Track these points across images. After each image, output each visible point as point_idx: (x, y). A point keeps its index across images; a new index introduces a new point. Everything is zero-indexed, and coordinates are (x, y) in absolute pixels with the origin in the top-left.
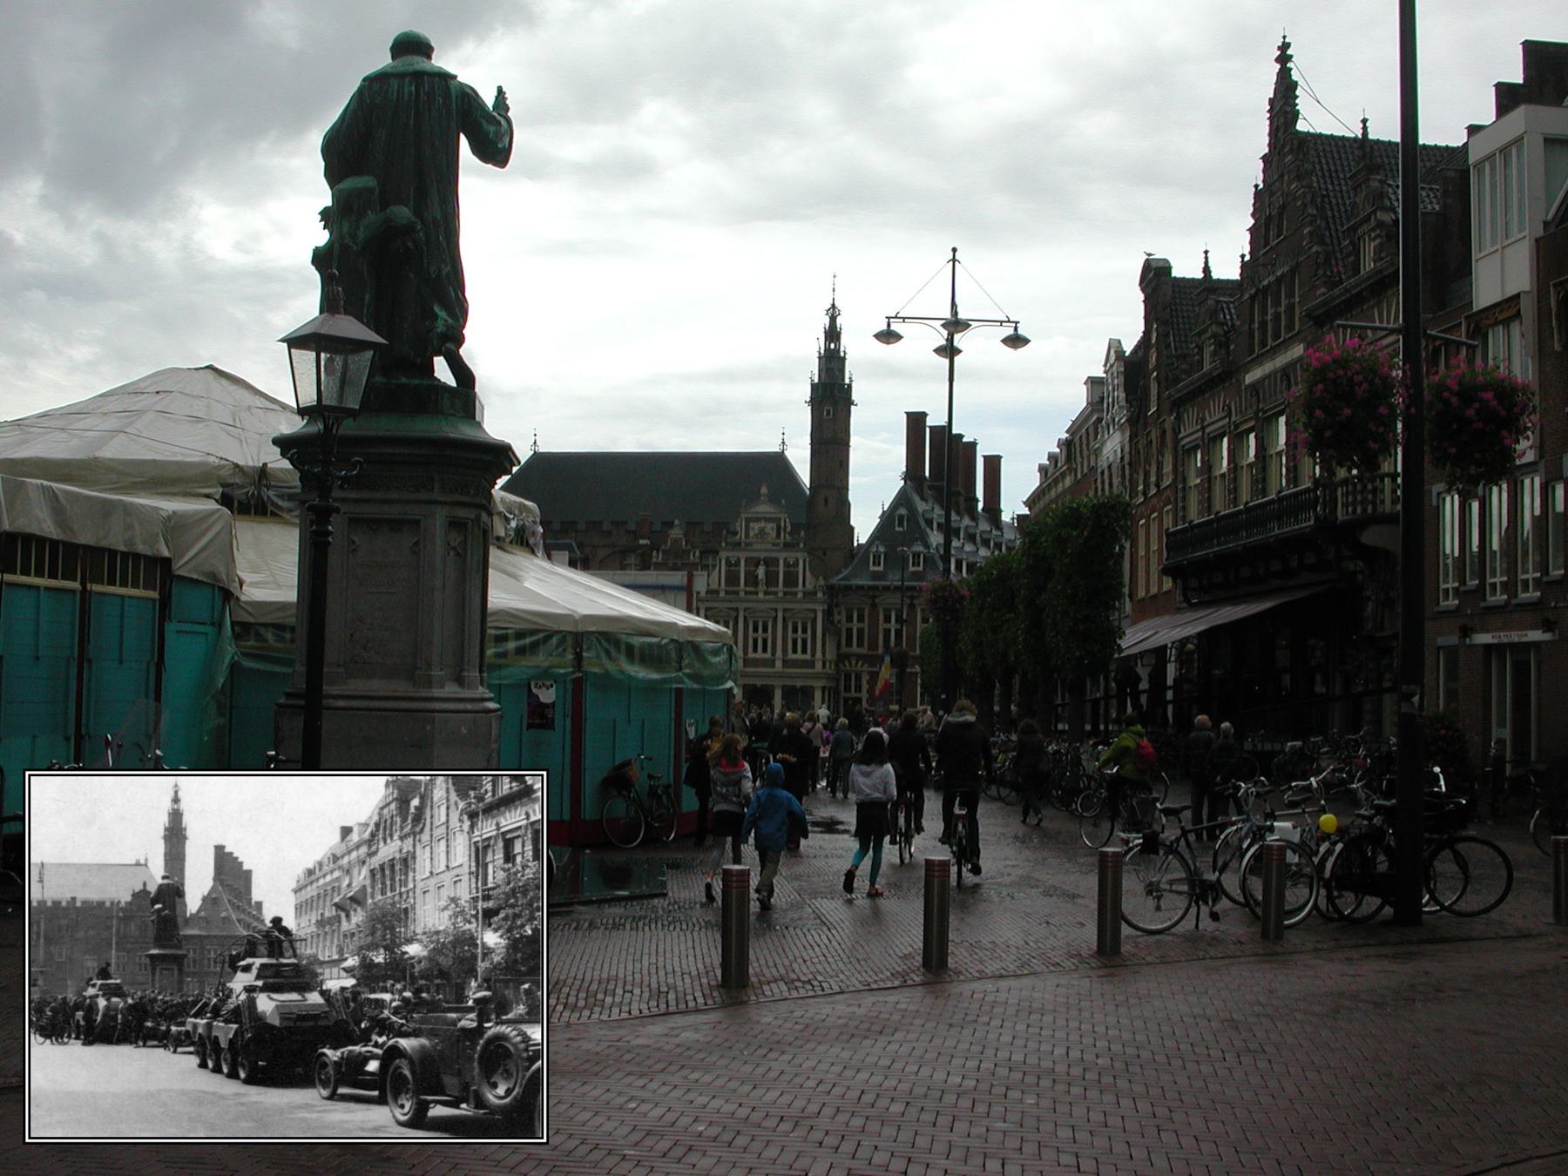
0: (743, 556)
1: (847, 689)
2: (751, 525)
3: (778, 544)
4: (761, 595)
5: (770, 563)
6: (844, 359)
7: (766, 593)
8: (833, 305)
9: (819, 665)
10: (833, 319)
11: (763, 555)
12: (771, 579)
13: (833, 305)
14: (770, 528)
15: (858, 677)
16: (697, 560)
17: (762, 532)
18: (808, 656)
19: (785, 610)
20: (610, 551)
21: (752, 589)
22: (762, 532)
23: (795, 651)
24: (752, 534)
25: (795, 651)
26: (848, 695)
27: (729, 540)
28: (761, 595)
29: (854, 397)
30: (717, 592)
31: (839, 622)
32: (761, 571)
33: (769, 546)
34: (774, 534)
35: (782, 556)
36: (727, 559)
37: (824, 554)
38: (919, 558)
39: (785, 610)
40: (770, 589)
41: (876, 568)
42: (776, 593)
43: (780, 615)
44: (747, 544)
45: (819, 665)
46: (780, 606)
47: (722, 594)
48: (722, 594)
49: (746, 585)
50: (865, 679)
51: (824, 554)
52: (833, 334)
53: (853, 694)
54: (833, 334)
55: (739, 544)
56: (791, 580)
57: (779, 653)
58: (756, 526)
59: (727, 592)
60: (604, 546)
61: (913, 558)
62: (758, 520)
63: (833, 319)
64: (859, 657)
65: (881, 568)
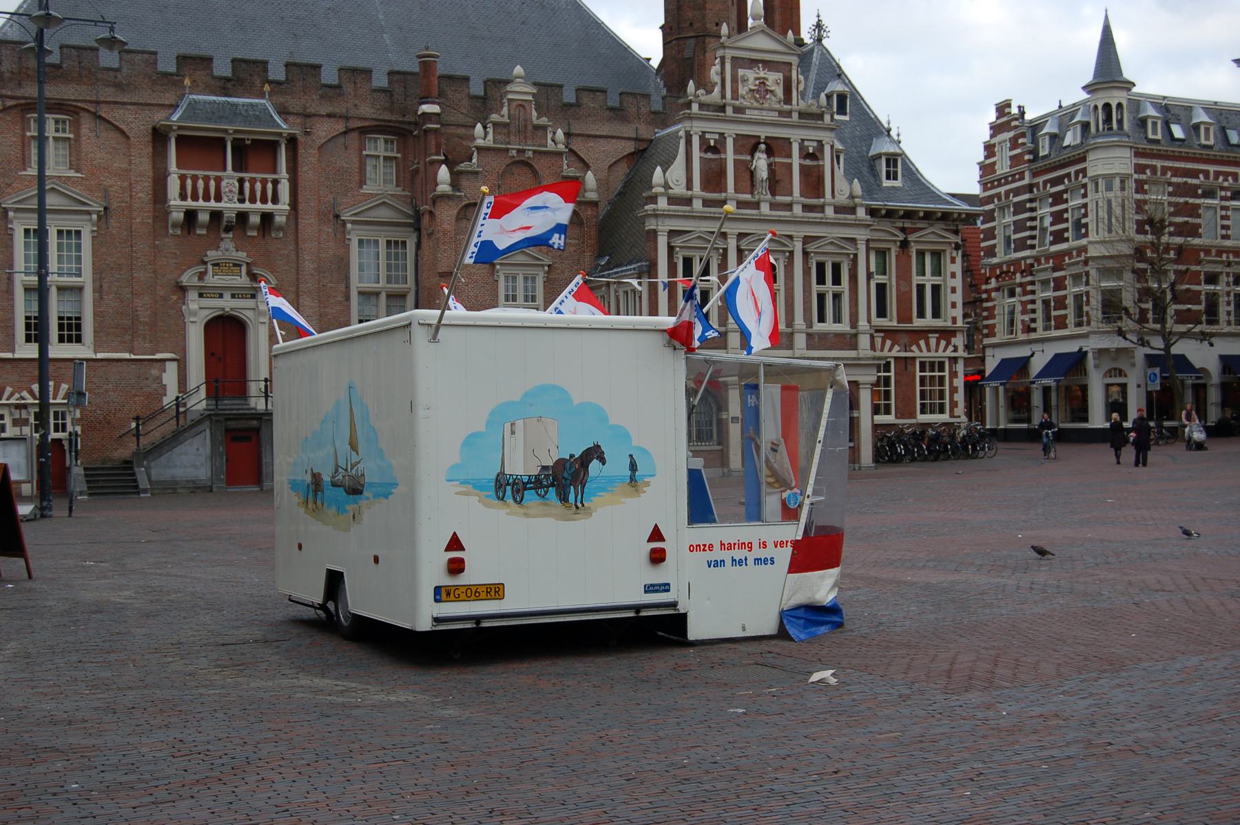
0: (731, 130)
2: (741, 72)
3: (789, 114)
4: (765, 209)
5: (774, 147)
7: (774, 206)
9: (864, 341)
11: (763, 132)
12: (776, 182)
14: (774, 79)
16: (561, 147)
17: (762, 88)
18: (844, 327)
19: (807, 240)
20: (340, 127)
21: (747, 197)
22: (762, 88)
23: (822, 319)
24: (742, 91)
25: (822, 319)
27: (705, 99)
28: (765, 209)
30: (688, 201)
32: (761, 163)
33: (774, 116)
34: (780, 92)
35: (795, 135)
36: (702, 138)
39: (807, 240)
40: (779, 198)
42: (789, 206)
43: (798, 247)
44: (738, 110)
45: (864, 341)
46: (800, 232)
47: (697, 205)
48: (697, 205)
49: (736, 191)
55: (722, 108)
56: (814, 182)
57: (799, 321)
58: (750, 74)
59: (706, 203)
60: (329, 116)
62: (753, 63)
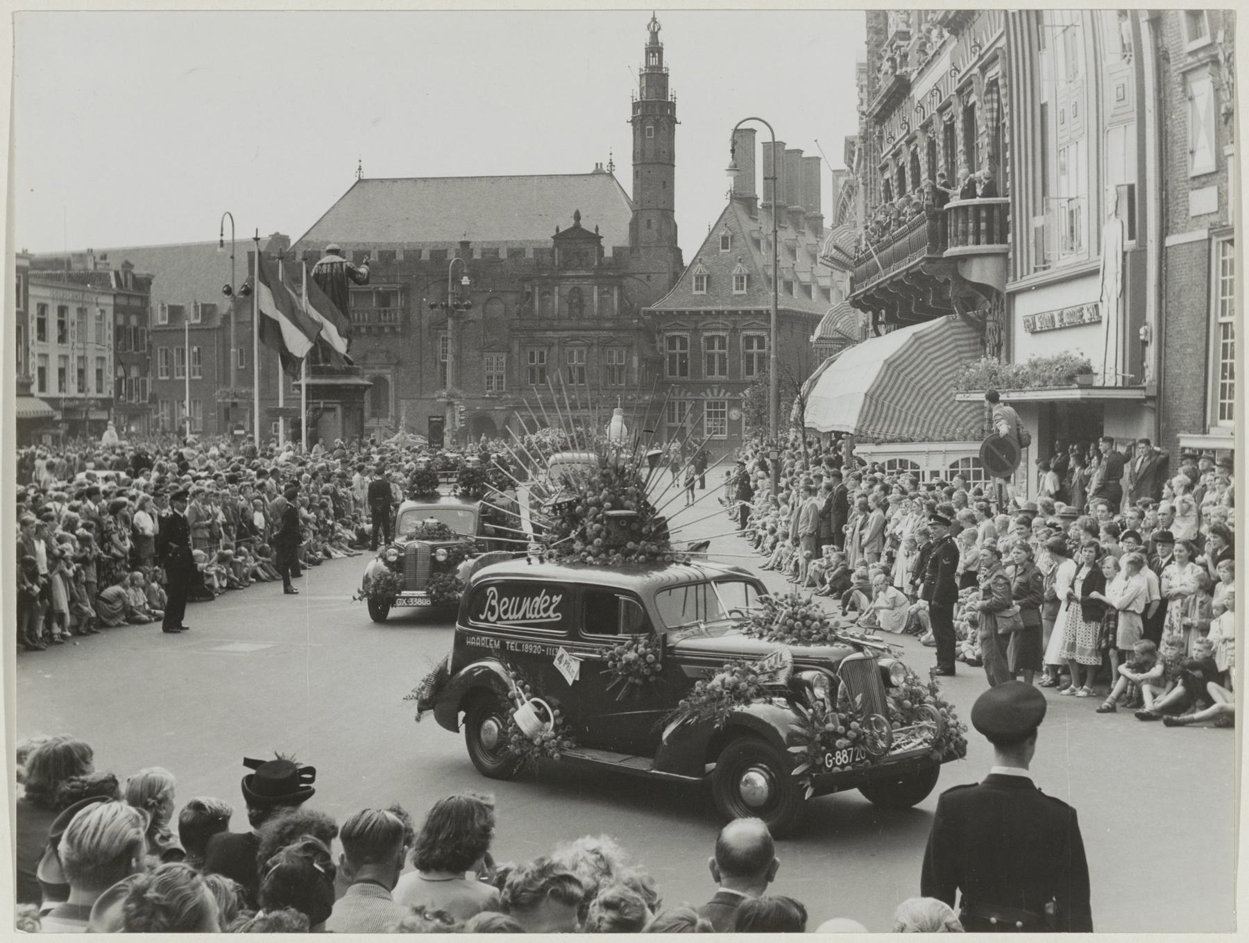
1: (671, 419)
6: (667, 75)
8: (654, 20)
10: (654, 35)
13: (654, 20)
15: (682, 406)
26: (672, 424)
29: (679, 115)
31: (661, 349)
37: (648, 277)
38: (742, 281)
41: (700, 292)
50: (688, 407)
51: (648, 277)
52: (655, 49)
53: (677, 424)
54: (655, 49)
61: (737, 281)
63: (654, 35)
64: (683, 384)
65: (704, 292)
